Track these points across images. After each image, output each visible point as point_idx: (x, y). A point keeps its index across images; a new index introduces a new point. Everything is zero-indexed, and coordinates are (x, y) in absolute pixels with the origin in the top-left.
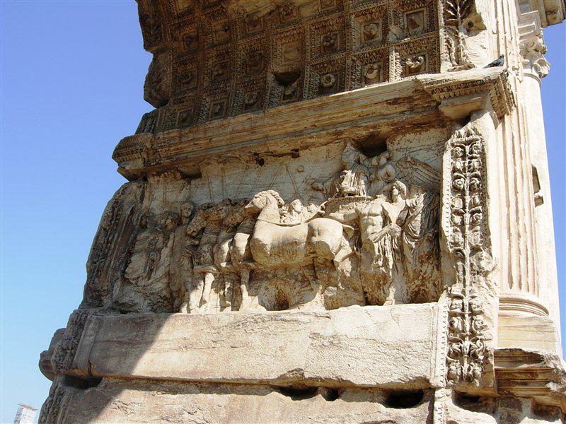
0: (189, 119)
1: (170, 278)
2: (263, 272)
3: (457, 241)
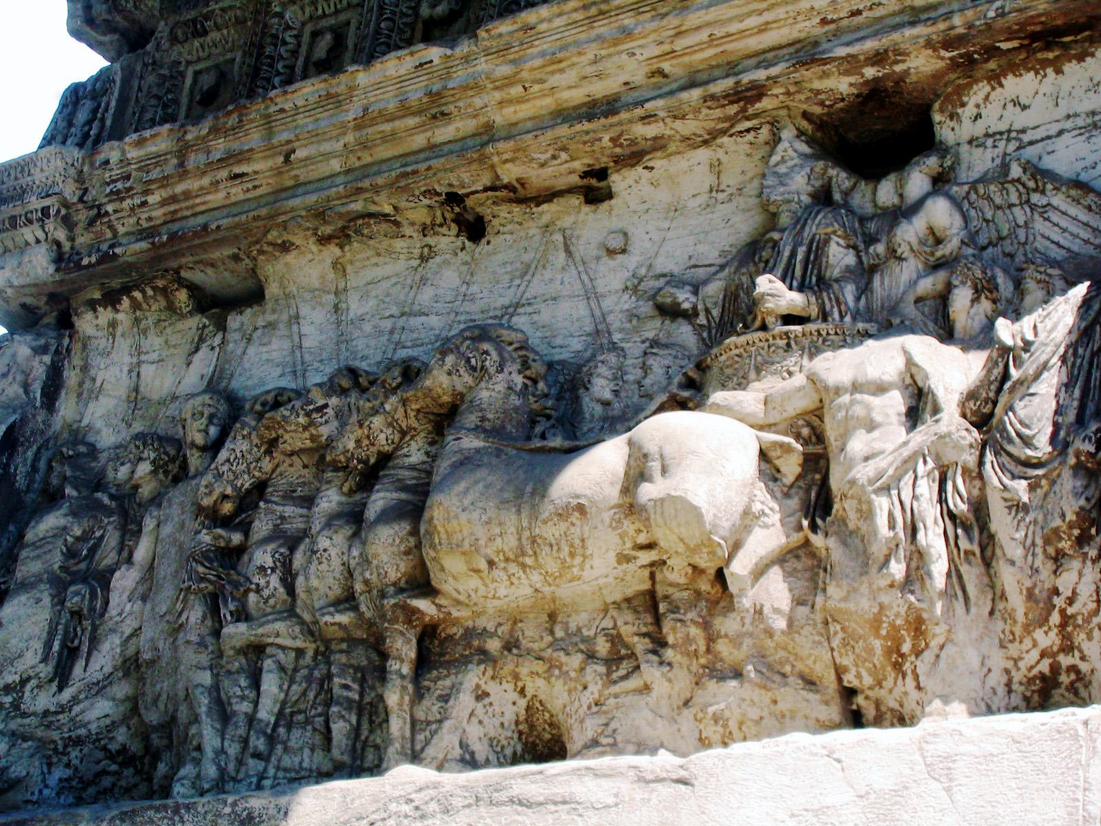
2: (469, 633)
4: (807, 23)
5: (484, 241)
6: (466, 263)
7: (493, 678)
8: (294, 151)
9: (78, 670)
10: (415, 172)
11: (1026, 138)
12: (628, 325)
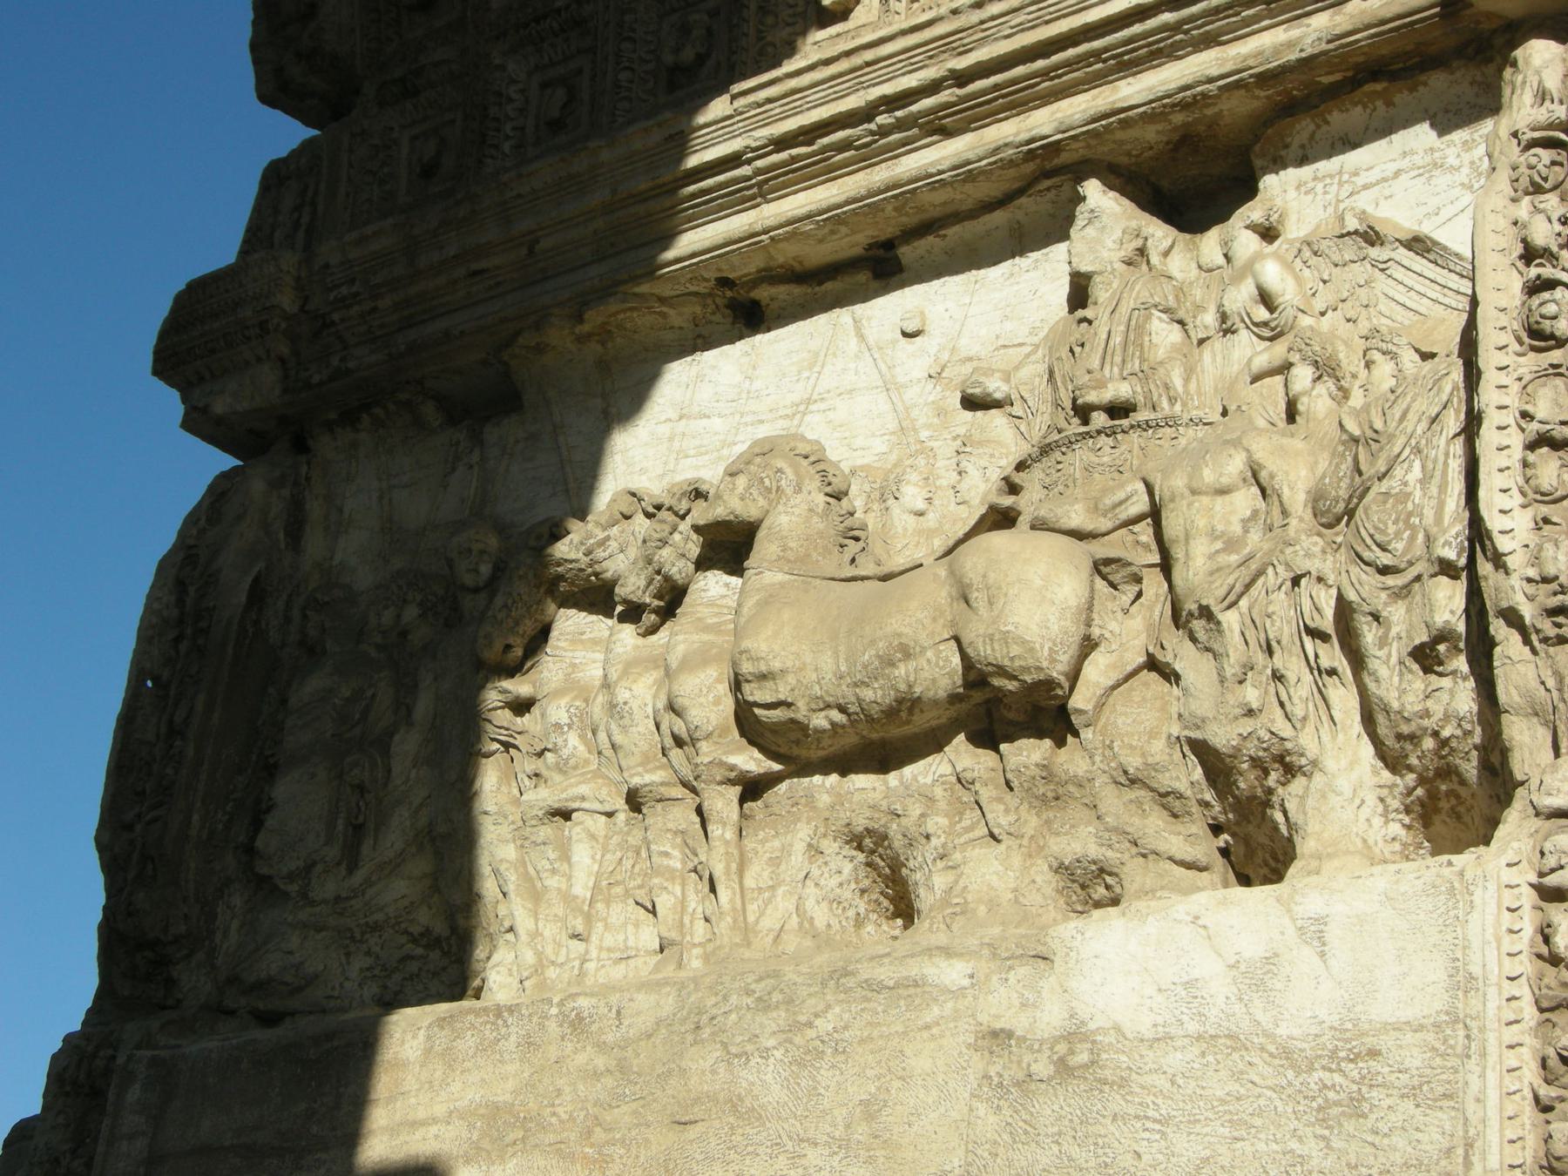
3: (1551, 570)
7: (825, 835)
8: (537, 241)
9: (366, 849)
11: (1360, 181)
12: (936, 420)
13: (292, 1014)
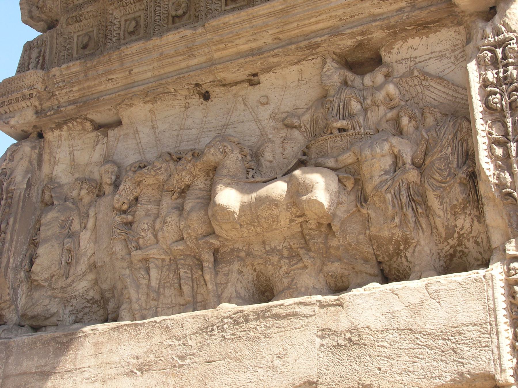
0: (92, 45)
1: (98, 273)
2: (232, 251)
4: (334, 20)
5: (210, 100)
6: (204, 109)
7: (244, 266)
8: (132, 70)
10: (183, 77)
11: (417, 60)
13: (45, 326)
